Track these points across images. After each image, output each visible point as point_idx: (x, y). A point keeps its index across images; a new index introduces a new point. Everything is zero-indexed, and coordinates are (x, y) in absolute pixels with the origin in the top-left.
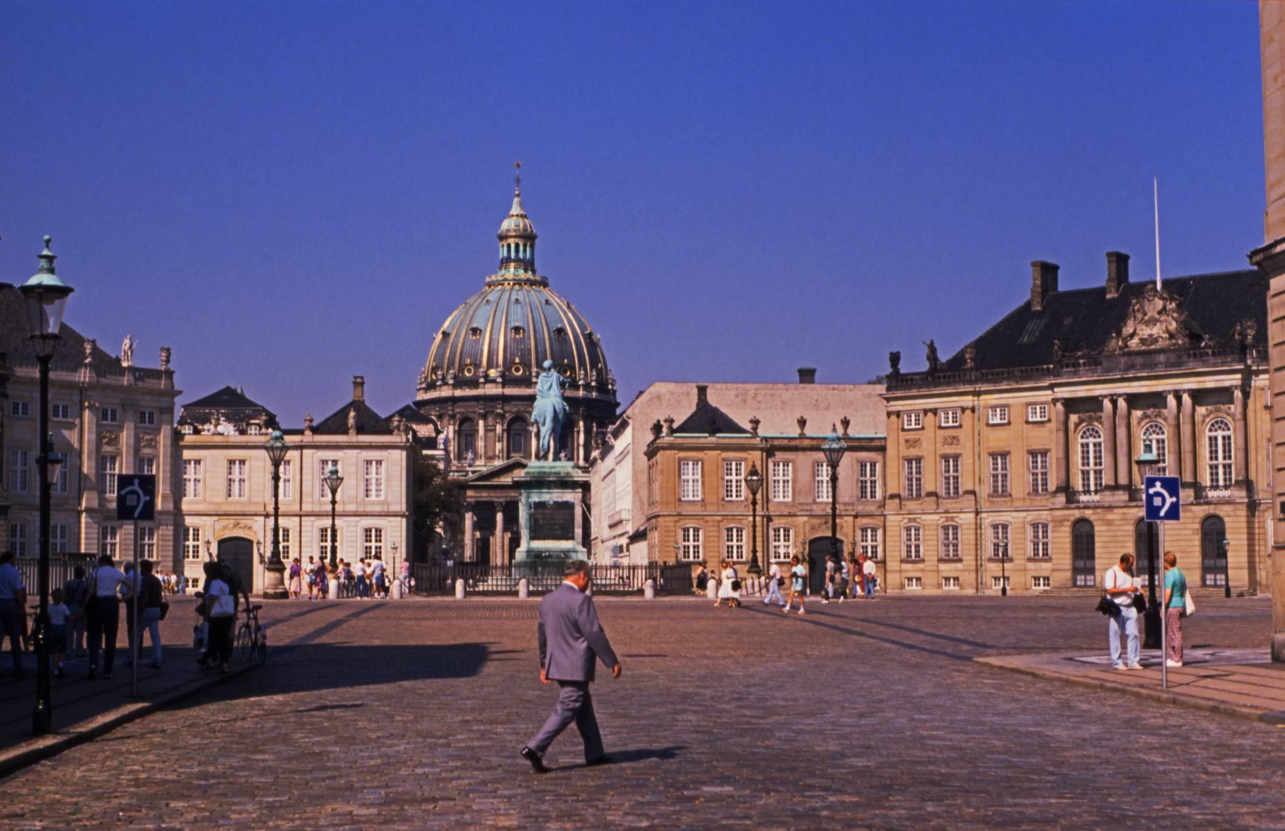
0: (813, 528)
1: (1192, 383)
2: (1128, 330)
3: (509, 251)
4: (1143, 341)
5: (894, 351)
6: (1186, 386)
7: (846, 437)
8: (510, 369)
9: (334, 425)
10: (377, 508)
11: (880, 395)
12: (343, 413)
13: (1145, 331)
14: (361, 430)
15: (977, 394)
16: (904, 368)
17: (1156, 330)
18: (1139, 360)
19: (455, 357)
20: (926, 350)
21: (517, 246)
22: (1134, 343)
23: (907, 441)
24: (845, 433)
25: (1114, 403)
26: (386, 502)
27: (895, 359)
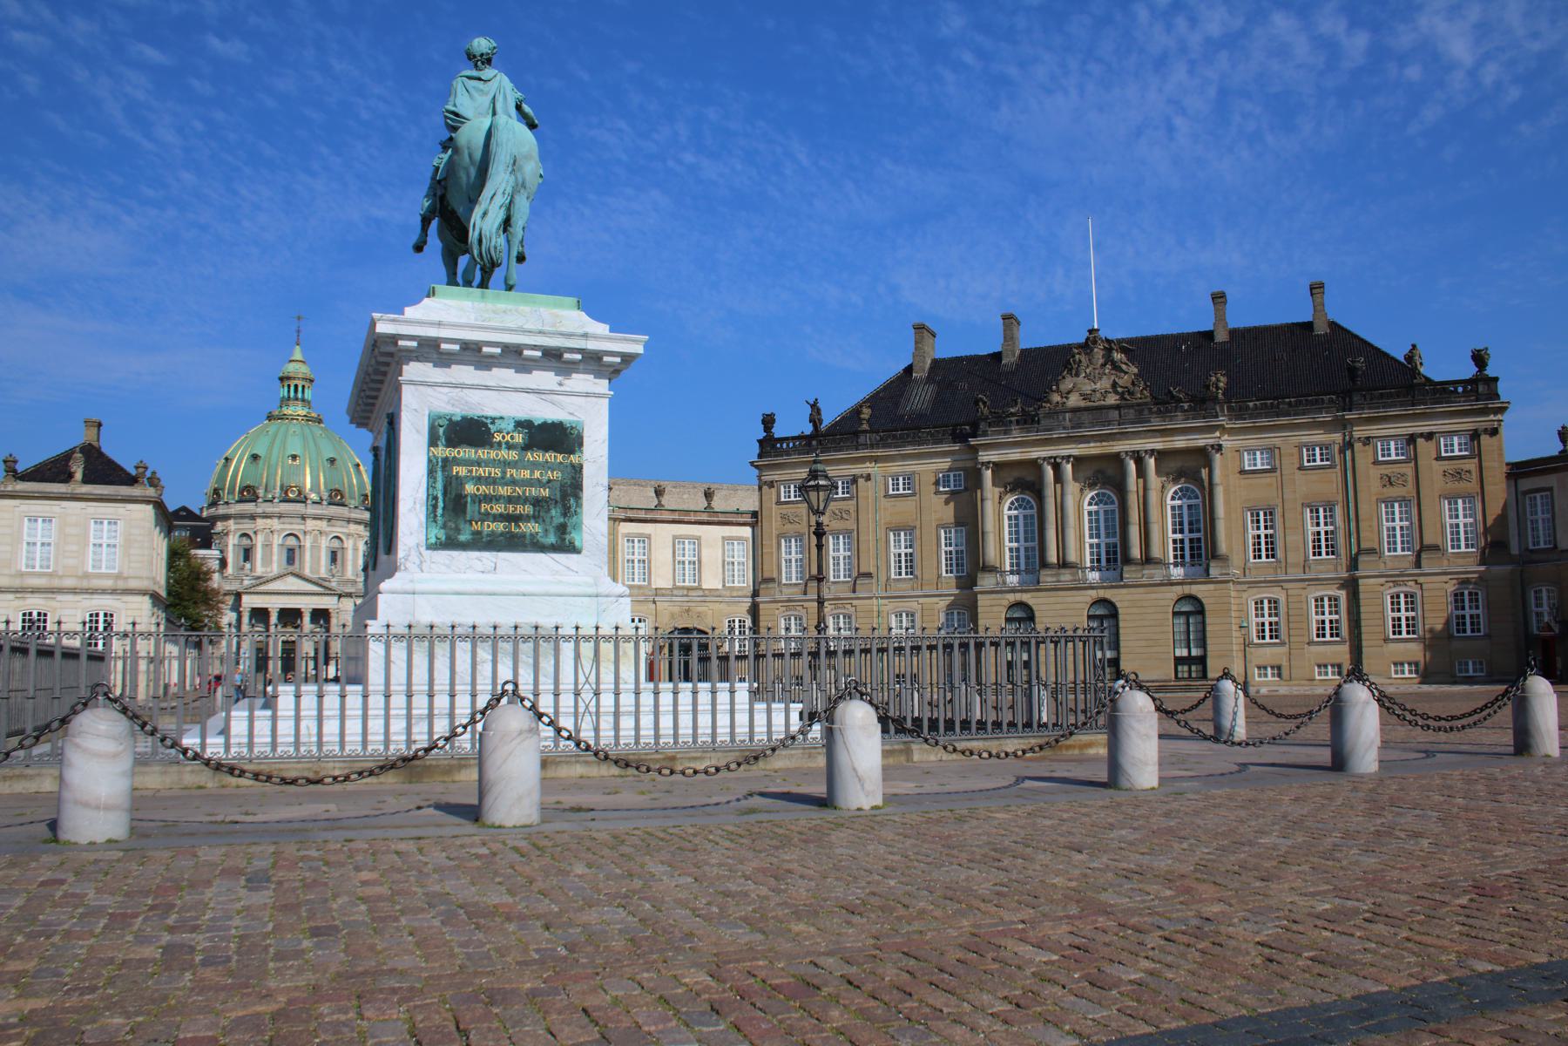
0: (672, 616)
1: (1158, 444)
2: (1068, 383)
3: (289, 391)
4: (1085, 397)
5: (769, 413)
6: (1149, 446)
7: (709, 509)
8: (286, 493)
9: (54, 471)
10: (108, 583)
11: (752, 463)
12: (67, 457)
13: (1088, 387)
14: (87, 480)
15: (876, 460)
16: (779, 431)
17: (1104, 384)
18: (1086, 417)
19: (238, 471)
20: (809, 410)
21: (296, 386)
22: (1074, 400)
23: (784, 518)
24: (709, 505)
25: (1057, 468)
26: (118, 577)
27: (768, 422)
